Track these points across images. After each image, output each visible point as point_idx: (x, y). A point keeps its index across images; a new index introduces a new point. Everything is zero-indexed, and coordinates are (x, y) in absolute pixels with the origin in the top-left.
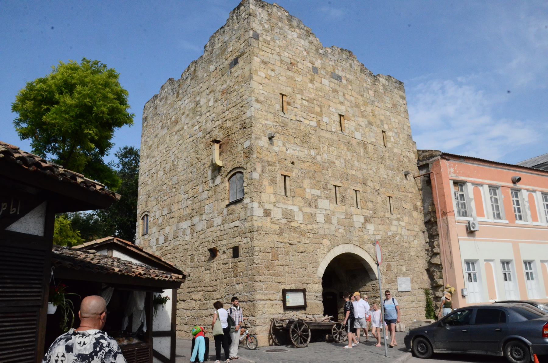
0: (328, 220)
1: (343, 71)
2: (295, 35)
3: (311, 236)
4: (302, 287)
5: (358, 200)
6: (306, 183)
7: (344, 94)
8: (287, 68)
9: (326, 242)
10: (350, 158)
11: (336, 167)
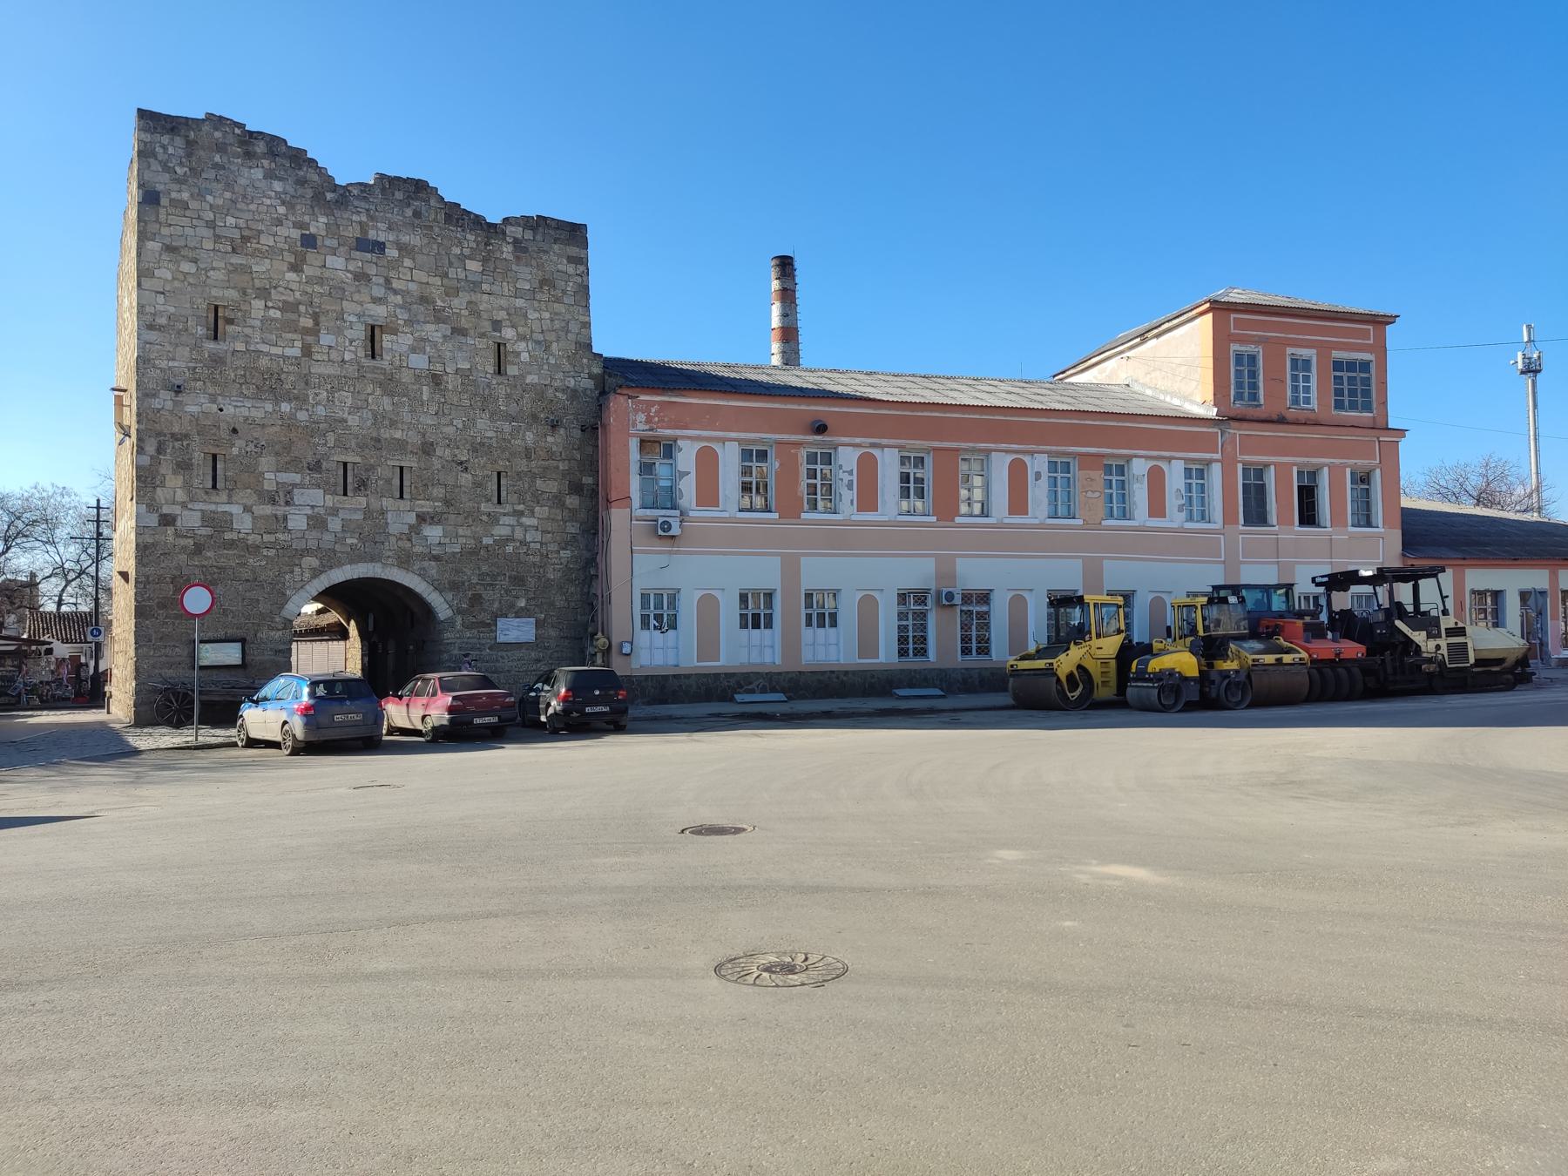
0: (317, 522)
1: (390, 228)
2: (258, 174)
3: (272, 553)
4: (240, 633)
5: (406, 483)
6: (266, 462)
7: (388, 281)
8: (229, 249)
9: (311, 561)
10: (389, 408)
11: (348, 428)
